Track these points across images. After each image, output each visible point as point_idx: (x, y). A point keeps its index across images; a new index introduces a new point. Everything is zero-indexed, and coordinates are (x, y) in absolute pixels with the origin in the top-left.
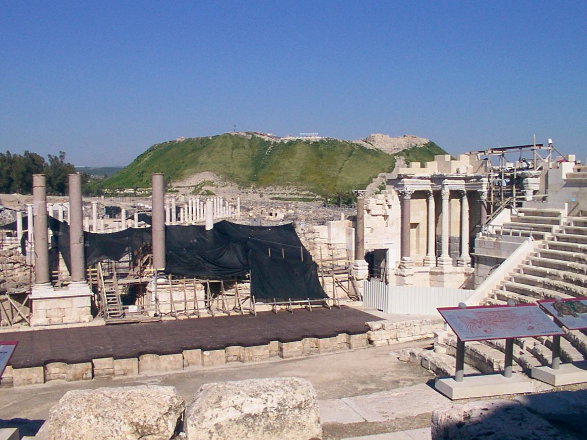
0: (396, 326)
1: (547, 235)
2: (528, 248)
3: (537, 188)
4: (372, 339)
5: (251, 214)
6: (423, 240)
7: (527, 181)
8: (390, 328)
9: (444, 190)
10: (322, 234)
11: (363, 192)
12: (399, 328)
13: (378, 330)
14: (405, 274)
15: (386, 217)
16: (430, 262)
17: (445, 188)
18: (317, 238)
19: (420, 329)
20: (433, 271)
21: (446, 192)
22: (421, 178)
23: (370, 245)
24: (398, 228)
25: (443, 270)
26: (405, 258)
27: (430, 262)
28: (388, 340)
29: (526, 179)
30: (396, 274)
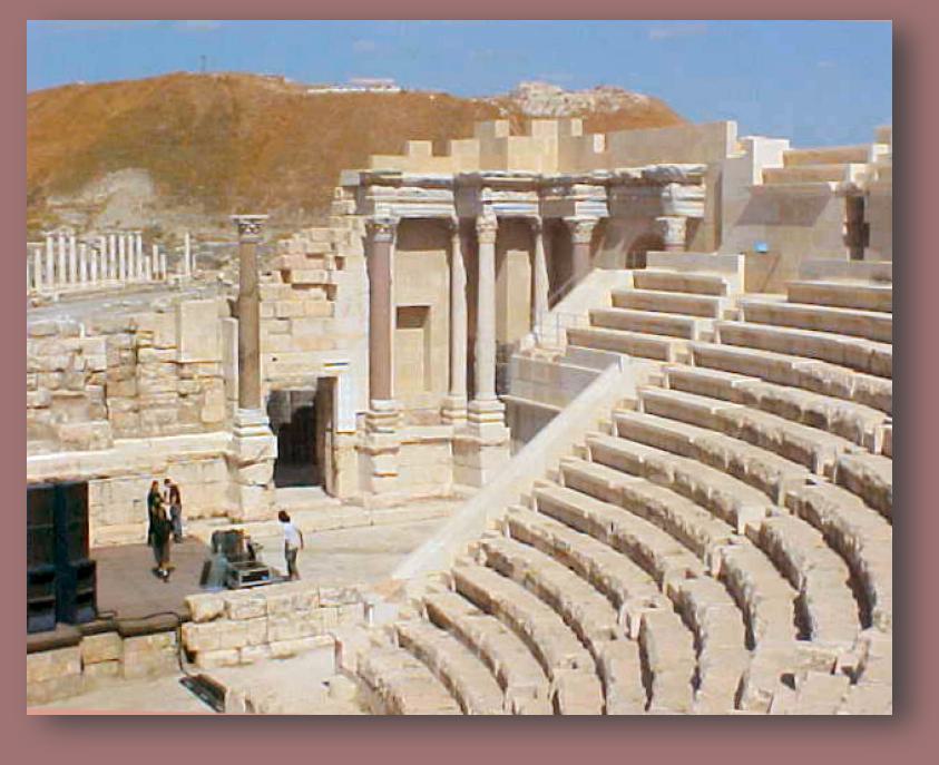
0: (265, 607)
1: (677, 346)
2: (622, 383)
3: (696, 211)
4: (194, 646)
5: (221, 275)
6: (439, 353)
7: (670, 192)
8: (245, 612)
9: (484, 217)
10: (161, 336)
11: (252, 221)
12: (273, 613)
13: (212, 620)
14: (374, 447)
15: (330, 290)
16: (454, 413)
17: (485, 212)
18: (147, 346)
19: (339, 615)
20: (458, 437)
21: (487, 221)
22: (426, 184)
23: (289, 364)
24: (361, 321)
25: (479, 435)
26: (378, 403)
27: (454, 413)
28: (239, 649)
29: (667, 188)
30: (356, 448)
